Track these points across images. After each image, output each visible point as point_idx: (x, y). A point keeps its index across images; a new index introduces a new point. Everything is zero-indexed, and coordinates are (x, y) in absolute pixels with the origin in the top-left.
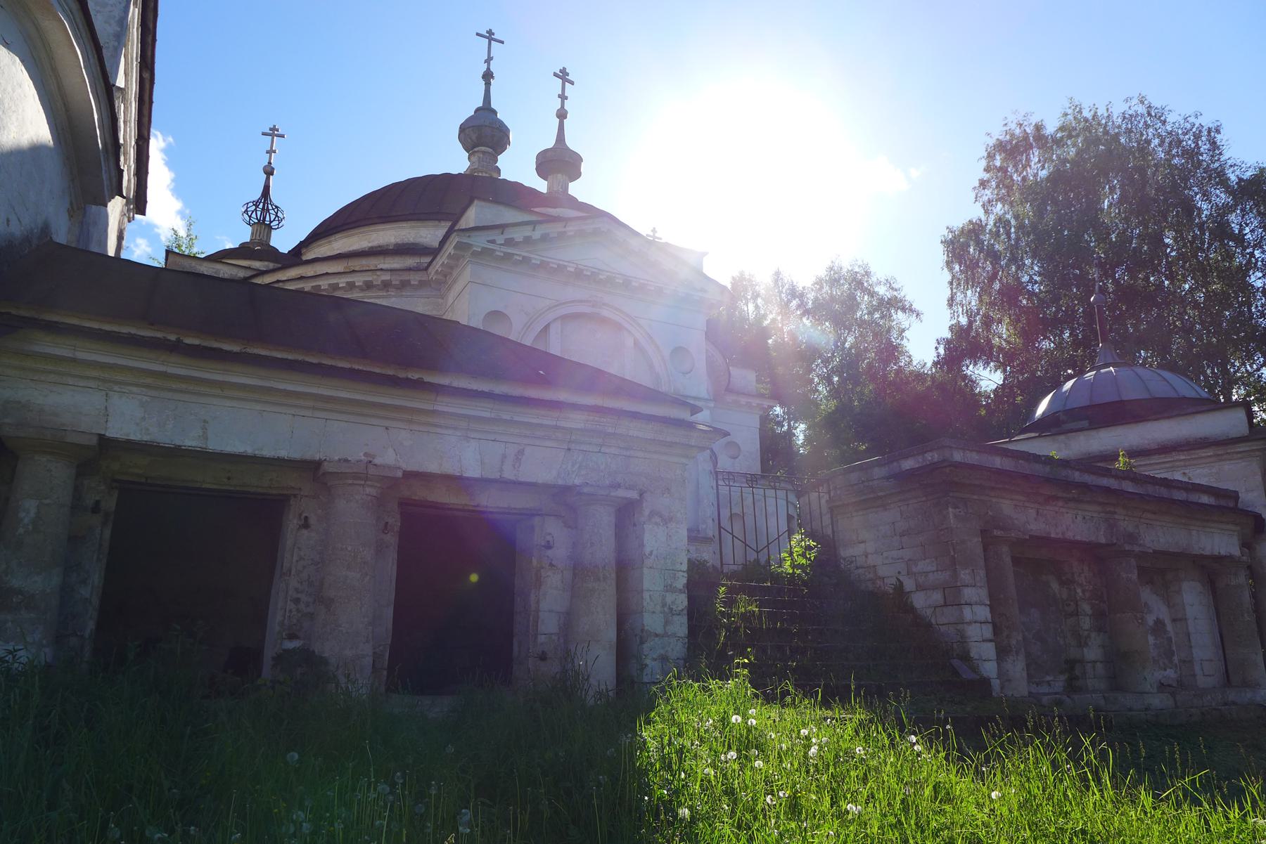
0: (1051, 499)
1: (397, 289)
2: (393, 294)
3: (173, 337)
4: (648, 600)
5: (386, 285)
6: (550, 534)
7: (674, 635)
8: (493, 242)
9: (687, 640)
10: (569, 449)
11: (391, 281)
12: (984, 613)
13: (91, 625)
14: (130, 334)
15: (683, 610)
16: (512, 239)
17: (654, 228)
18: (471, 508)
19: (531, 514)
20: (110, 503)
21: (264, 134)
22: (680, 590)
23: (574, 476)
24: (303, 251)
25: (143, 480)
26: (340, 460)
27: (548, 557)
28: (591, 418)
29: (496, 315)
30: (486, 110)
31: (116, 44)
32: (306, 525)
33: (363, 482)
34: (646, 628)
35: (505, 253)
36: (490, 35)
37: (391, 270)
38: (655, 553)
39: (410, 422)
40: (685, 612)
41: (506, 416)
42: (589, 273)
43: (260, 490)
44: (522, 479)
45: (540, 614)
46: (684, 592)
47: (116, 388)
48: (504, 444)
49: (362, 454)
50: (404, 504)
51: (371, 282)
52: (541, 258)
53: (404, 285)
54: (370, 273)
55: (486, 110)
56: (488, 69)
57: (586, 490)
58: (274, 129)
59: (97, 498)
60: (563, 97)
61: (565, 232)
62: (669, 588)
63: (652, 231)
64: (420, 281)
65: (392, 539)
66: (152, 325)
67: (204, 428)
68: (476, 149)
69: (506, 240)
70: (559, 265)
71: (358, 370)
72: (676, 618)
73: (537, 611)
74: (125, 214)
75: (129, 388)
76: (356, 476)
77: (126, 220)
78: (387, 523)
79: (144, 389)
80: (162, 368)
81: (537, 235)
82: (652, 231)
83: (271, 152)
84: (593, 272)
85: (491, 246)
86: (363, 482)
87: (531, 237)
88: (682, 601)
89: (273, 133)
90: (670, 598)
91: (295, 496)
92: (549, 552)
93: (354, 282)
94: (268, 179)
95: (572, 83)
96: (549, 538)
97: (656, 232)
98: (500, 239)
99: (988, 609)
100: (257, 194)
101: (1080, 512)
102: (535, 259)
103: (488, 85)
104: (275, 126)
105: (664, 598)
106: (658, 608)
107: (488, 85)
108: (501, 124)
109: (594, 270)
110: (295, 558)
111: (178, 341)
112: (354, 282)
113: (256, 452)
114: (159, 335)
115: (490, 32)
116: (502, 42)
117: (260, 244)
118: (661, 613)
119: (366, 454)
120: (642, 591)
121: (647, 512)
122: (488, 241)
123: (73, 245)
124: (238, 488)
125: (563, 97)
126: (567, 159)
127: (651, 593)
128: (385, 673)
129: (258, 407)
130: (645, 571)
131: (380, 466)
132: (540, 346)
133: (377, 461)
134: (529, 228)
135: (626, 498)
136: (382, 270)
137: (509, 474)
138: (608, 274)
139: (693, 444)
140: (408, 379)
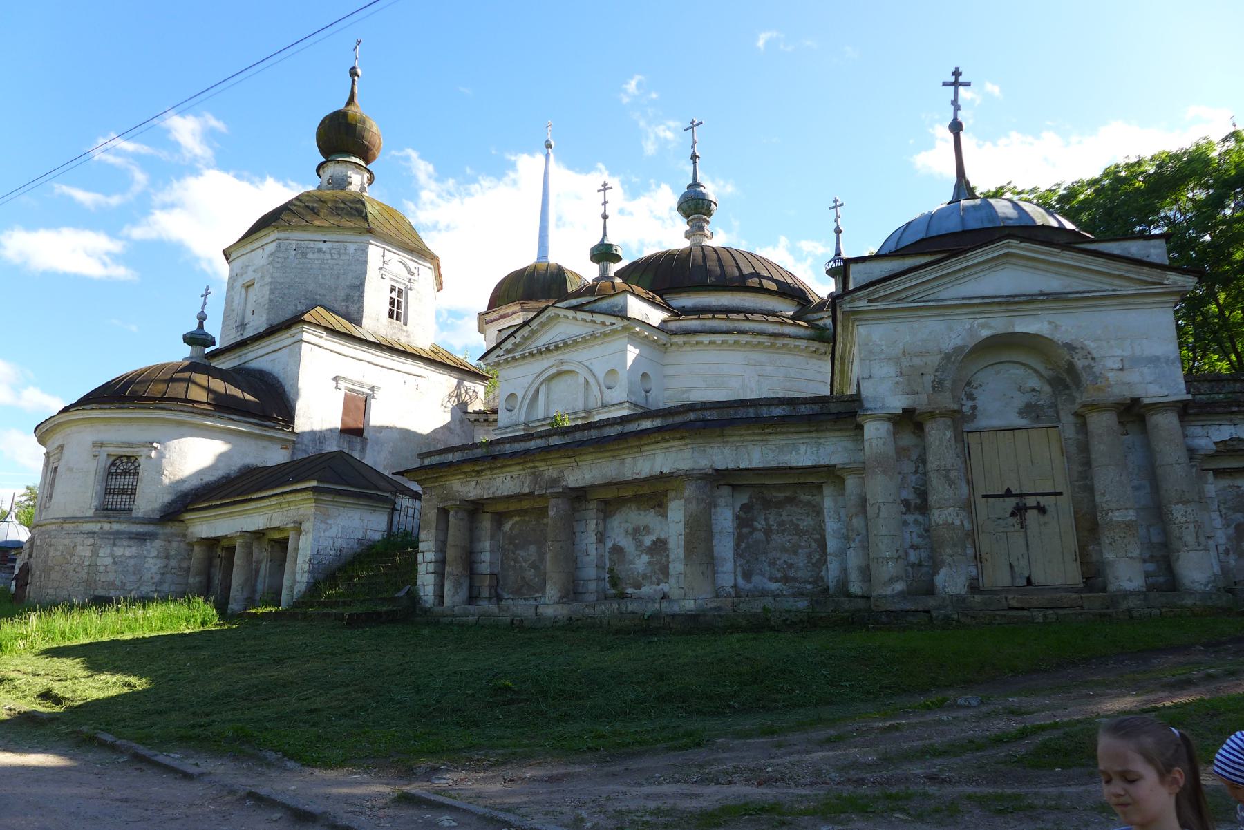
0: (479, 472)
8: (498, 356)
12: (430, 556)
55: (695, 184)
81: (518, 340)
85: (497, 359)
99: (433, 554)
101: (508, 474)
103: (695, 163)
107: (695, 163)
134: (512, 338)
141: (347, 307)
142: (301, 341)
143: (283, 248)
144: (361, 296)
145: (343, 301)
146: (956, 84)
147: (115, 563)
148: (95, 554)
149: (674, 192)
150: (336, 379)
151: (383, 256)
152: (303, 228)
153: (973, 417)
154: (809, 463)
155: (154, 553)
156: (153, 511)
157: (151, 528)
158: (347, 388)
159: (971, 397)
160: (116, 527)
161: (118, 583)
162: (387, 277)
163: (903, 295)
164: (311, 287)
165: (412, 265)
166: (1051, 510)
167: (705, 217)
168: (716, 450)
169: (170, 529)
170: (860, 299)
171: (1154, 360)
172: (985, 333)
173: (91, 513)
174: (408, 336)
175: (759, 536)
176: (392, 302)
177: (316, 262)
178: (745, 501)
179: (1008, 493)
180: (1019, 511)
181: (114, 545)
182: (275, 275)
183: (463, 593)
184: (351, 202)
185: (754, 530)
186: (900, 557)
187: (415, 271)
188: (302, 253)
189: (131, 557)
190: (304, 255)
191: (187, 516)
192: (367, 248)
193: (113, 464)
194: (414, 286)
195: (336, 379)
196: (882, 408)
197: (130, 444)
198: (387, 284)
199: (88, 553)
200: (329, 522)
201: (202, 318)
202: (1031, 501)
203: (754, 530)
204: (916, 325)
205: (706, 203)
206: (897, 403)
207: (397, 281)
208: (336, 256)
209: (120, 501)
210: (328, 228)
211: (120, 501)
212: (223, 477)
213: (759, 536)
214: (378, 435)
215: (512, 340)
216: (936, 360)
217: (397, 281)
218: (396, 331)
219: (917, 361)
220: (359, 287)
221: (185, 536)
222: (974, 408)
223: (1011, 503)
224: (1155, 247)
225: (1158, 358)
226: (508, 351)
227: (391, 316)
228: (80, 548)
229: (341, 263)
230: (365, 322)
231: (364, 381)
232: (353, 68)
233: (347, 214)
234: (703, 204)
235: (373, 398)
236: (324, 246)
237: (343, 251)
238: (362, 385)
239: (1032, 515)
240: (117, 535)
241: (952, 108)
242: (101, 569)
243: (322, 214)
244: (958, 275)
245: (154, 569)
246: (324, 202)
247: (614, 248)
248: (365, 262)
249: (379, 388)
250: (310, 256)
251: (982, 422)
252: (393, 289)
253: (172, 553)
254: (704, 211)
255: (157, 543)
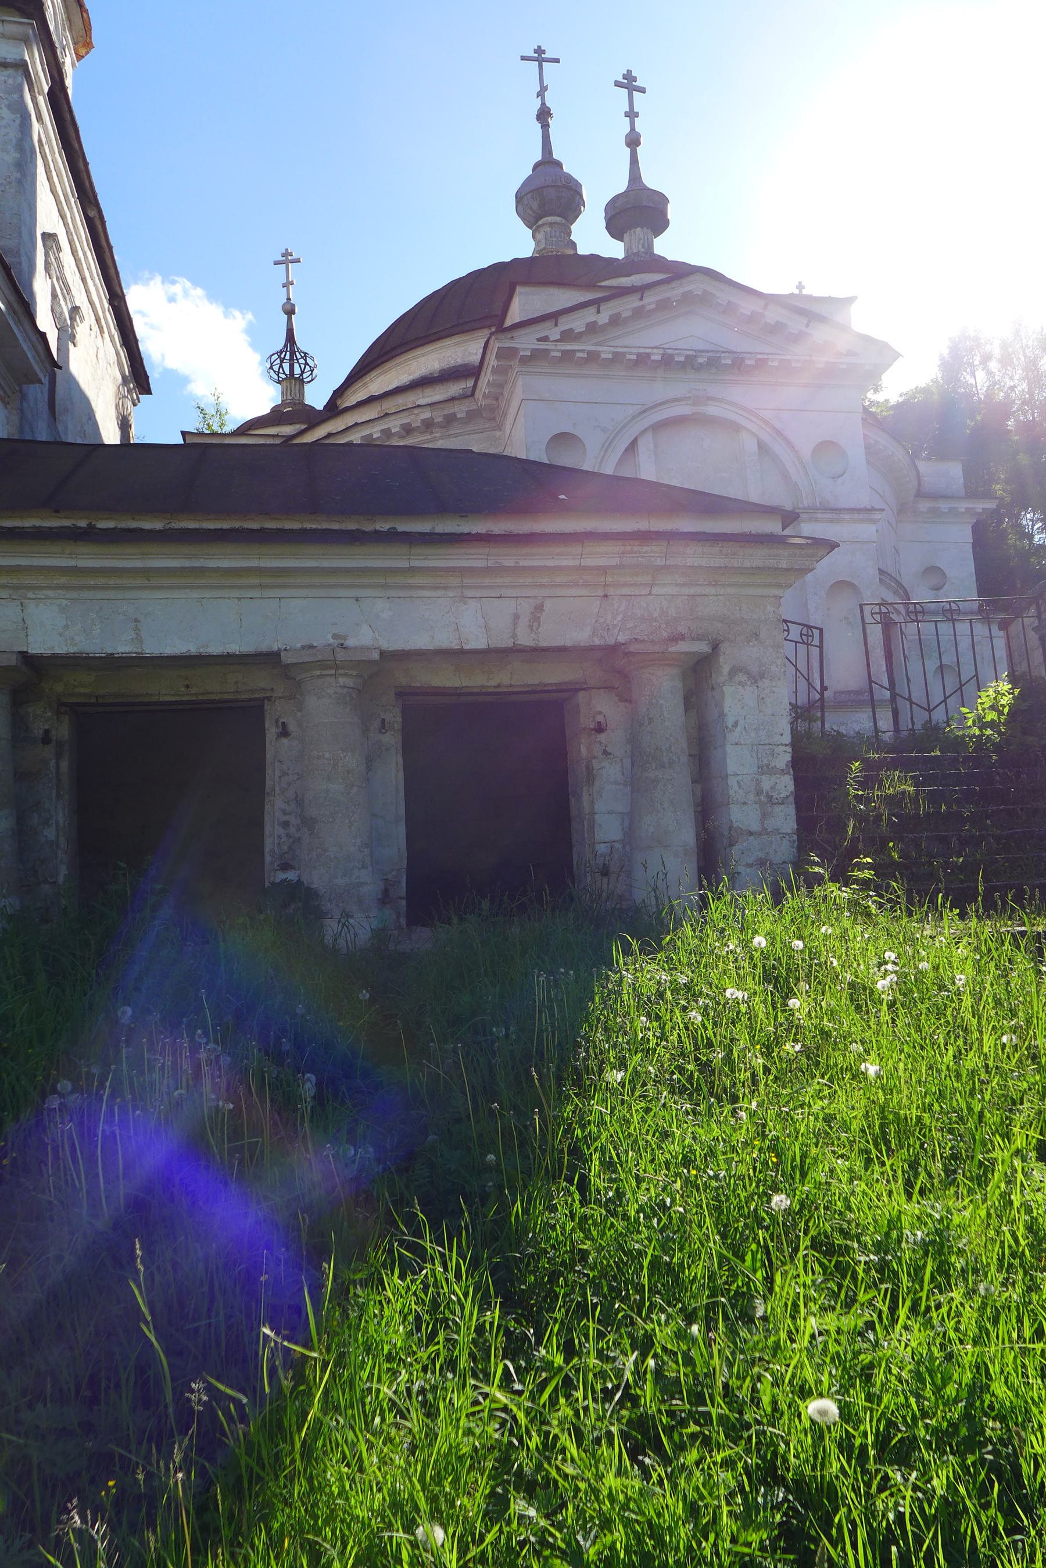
1: (443, 427)
2: (438, 435)
3: (83, 523)
4: (736, 787)
5: (428, 425)
6: (601, 713)
7: (777, 831)
8: (545, 339)
9: (795, 837)
10: (606, 596)
11: (432, 418)
13: (63, 870)
14: (34, 527)
15: (787, 797)
16: (571, 330)
17: (800, 283)
18: (490, 690)
19: (573, 689)
20: (63, 731)
21: (276, 263)
22: (782, 770)
23: (616, 631)
24: (339, 402)
25: (93, 700)
26: (303, 647)
27: (601, 743)
28: (628, 548)
29: (562, 439)
30: (548, 163)
31: (19, 175)
32: (284, 733)
33: (333, 672)
34: (735, 825)
35: (562, 351)
36: (540, 55)
37: (430, 405)
38: (741, 723)
39: (385, 586)
40: (792, 799)
41: (508, 563)
42: (682, 359)
43: (226, 697)
44: (544, 644)
45: (597, 817)
46: (789, 773)
47: (30, 595)
48: (513, 602)
49: (329, 636)
50: (402, 694)
51: (409, 424)
52: (636, 350)
53: (450, 420)
54: (406, 414)
55: (548, 163)
56: (543, 104)
57: (632, 648)
58: (286, 254)
59: (46, 727)
60: (632, 115)
61: (643, 306)
62: (766, 769)
63: (797, 287)
64: (468, 412)
65: (392, 739)
66: (57, 511)
67: (136, 629)
68: (540, 223)
69: (563, 333)
70: (639, 355)
71: (311, 530)
72: (778, 809)
73: (593, 813)
74: (124, 397)
75: (44, 592)
76: (322, 665)
77: (129, 404)
78: (383, 720)
79: (60, 592)
80: (71, 563)
81: (603, 318)
82: (797, 287)
83: (287, 285)
84: (687, 356)
85: (543, 346)
86: (333, 672)
87: (595, 322)
88: (786, 785)
89: (287, 259)
90: (766, 783)
91: (269, 699)
92: (602, 737)
93: (389, 429)
94: (290, 320)
95: (643, 90)
96: (600, 718)
97: (804, 287)
98: (555, 334)
100: (280, 342)
102: (605, 352)
103: (545, 127)
104: (287, 250)
105: (758, 782)
106: (752, 797)
107: (545, 127)
108: (569, 178)
109: (688, 353)
110: (277, 774)
111: (91, 526)
112: (389, 429)
113: (202, 650)
114: (67, 523)
115: (539, 51)
116: (557, 61)
117: (292, 404)
118: (756, 803)
119: (335, 636)
120: (727, 776)
121: (726, 669)
122: (539, 340)
123: (16, 437)
124: (200, 697)
125: (632, 115)
126: (645, 204)
127: (740, 778)
128: (404, 903)
129: (195, 594)
130: (729, 748)
131: (355, 648)
132: (627, 472)
133: (351, 642)
134: (592, 310)
135: (690, 653)
136: (419, 406)
137: (525, 639)
138: (710, 354)
139: (785, 566)
140: (376, 532)
215: (589, 315)
226: (568, 336)
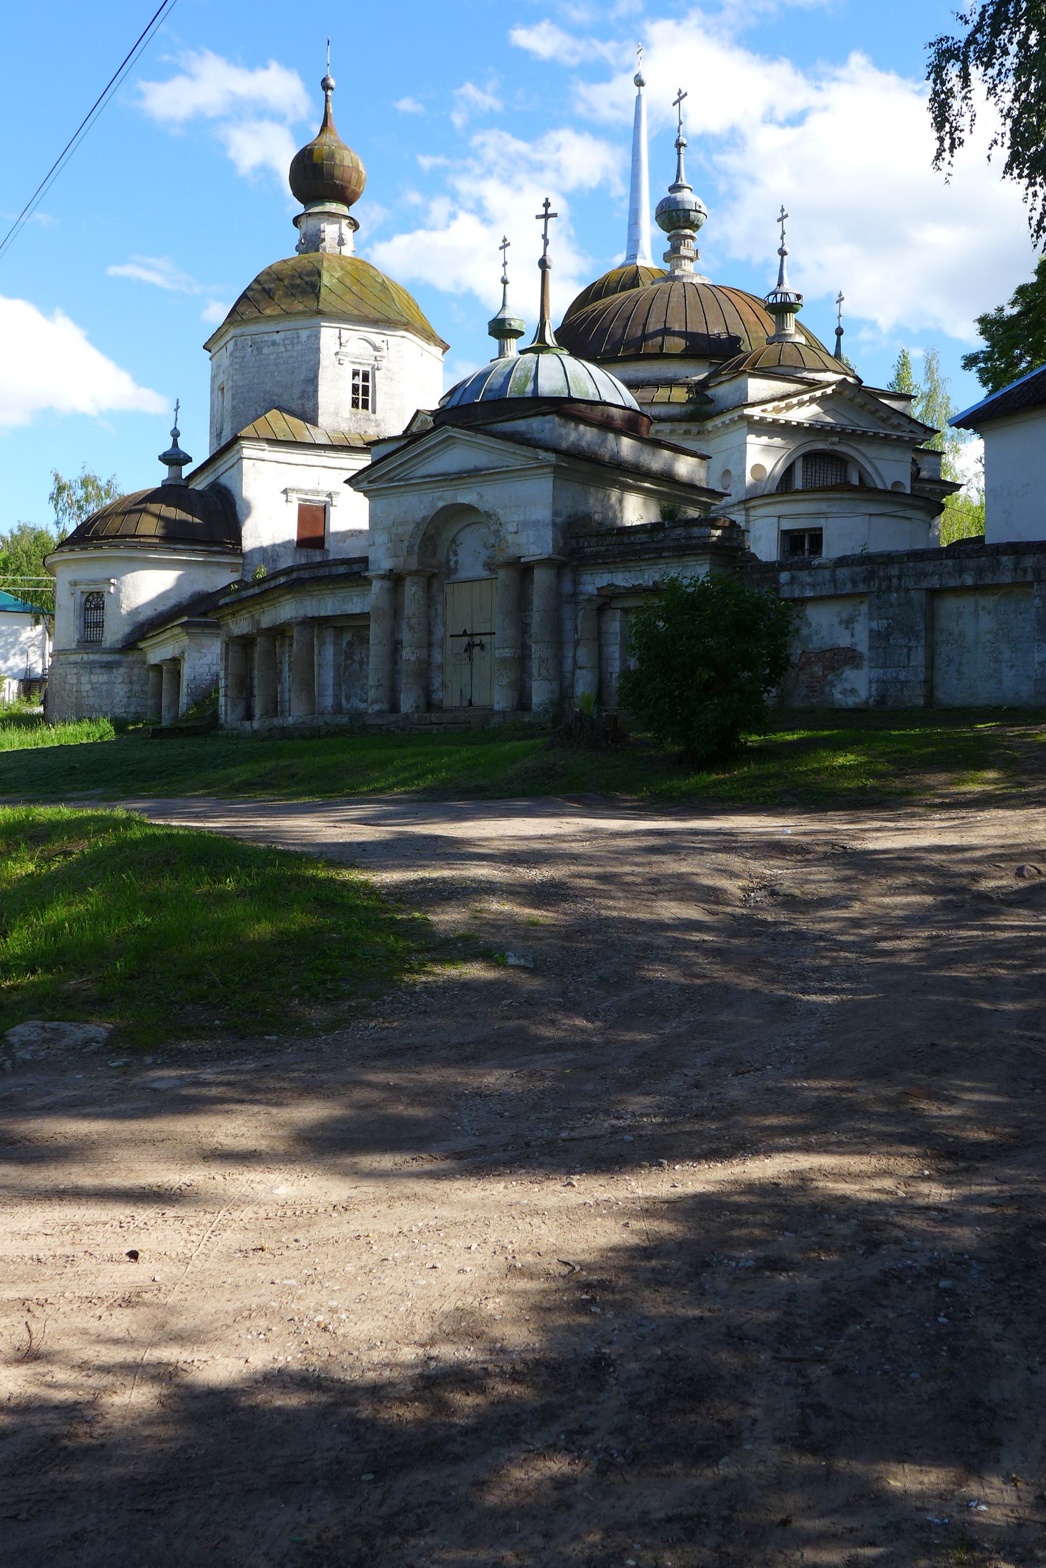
141: (303, 405)
142: (242, 458)
143: (240, 346)
144: (316, 391)
145: (299, 398)
146: (546, 216)
147: (93, 689)
148: (79, 683)
149: (904, 74)
150: (285, 492)
151: (340, 338)
152: (256, 320)
153: (456, 570)
154: (358, 611)
155: (120, 680)
156: (117, 641)
157: (116, 657)
158: (300, 499)
159: (455, 554)
160: (92, 657)
161: (97, 706)
162: (346, 361)
163: (392, 475)
164: (269, 387)
165: (377, 338)
166: (487, 646)
167: (688, 232)
168: (308, 602)
169: (132, 657)
170: (362, 481)
171: (536, 524)
172: (441, 504)
173: (74, 646)
174: (378, 426)
175: (356, 666)
176: (355, 389)
177: (272, 357)
178: (349, 639)
179: (465, 634)
180: (470, 647)
181: (91, 673)
182: (236, 377)
183: (240, 711)
184: (308, 275)
185: (354, 661)
186: (381, 685)
187: (384, 346)
188: (258, 349)
189: (103, 683)
190: (259, 350)
191: (142, 645)
192: (319, 332)
193: (87, 600)
194: (383, 364)
195: (285, 492)
196: (379, 569)
197: (94, 582)
198: (348, 369)
199: (75, 681)
200: (203, 651)
201: (175, 434)
202: (477, 640)
203: (354, 661)
204: (401, 499)
205: (681, 213)
206: (386, 564)
207: (360, 363)
208: (289, 348)
209: (92, 634)
210: (279, 316)
211: (92, 634)
212: (175, 606)
213: (356, 666)
214: (341, 544)
216: (411, 527)
217: (360, 363)
218: (362, 423)
219: (400, 530)
220: (312, 381)
221: (144, 663)
222: (456, 562)
223: (466, 640)
224: (548, 422)
225: (539, 521)
227: (355, 404)
228: (69, 676)
229: (295, 354)
230: (321, 420)
231: (320, 488)
232: (324, 80)
233: (301, 293)
234: (678, 216)
235: (332, 505)
236: (277, 337)
237: (295, 341)
238: (317, 493)
239: (477, 649)
240: (92, 663)
241: (548, 237)
242: (85, 694)
243: (276, 297)
244: (425, 455)
245: (122, 693)
246: (281, 280)
247: (507, 322)
248: (317, 350)
249: (338, 493)
250: (265, 351)
251: (462, 574)
252: (355, 374)
253: (135, 678)
254: (682, 224)
255: (122, 670)
